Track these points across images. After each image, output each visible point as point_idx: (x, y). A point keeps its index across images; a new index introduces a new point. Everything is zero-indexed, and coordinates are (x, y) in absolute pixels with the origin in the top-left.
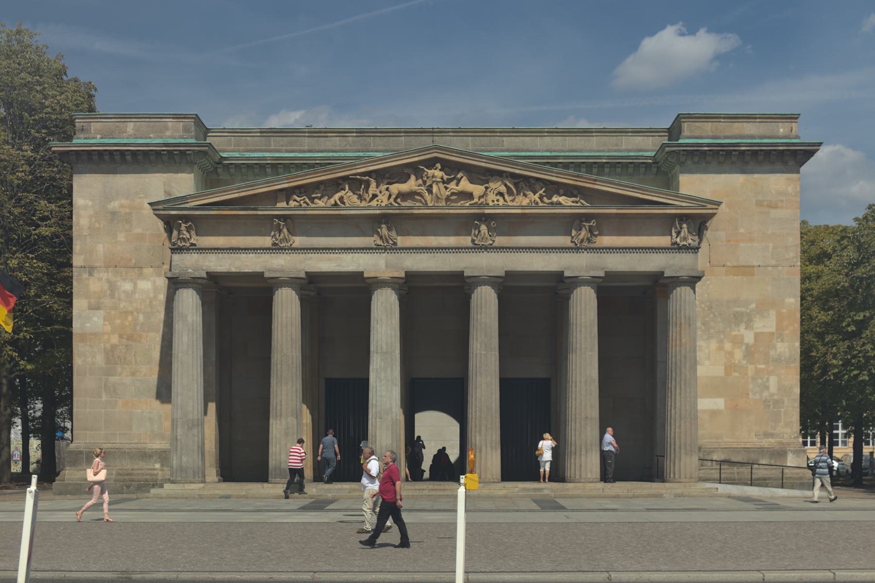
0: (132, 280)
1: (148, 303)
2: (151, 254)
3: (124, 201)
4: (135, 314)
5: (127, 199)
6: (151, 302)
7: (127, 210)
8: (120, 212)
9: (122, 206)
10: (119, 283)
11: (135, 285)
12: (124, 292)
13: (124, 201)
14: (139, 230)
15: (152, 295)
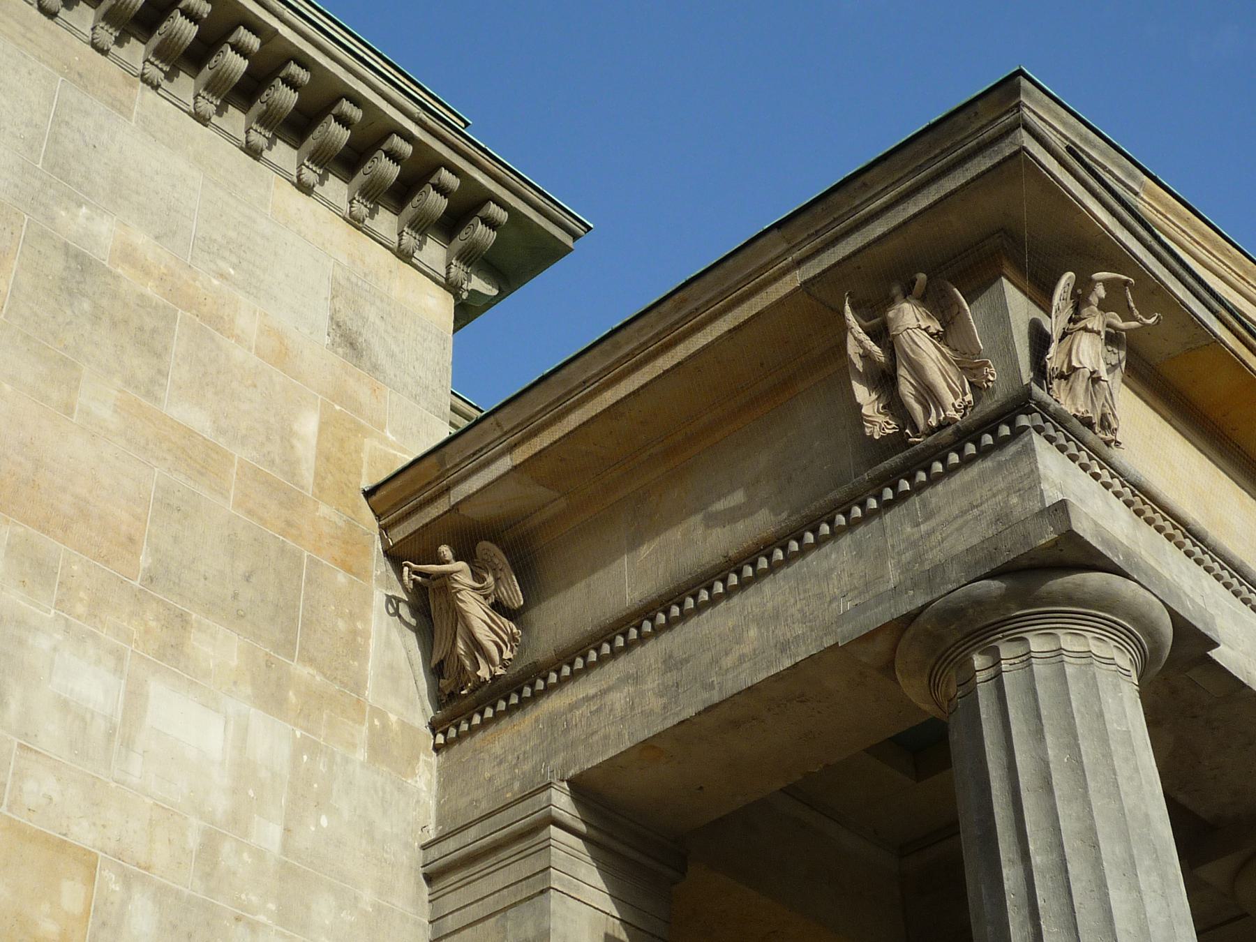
0: (119, 656)
1: (193, 841)
2: (242, 567)
3: (141, 240)
4: (109, 880)
5: (157, 238)
6: (210, 845)
7: (150, 289)
8: (117, 277)
9: (128, 255)
10: (42, 643)
11: (135, 697)
12: (64, 705)
13: (141, 240)
14: (198, 419)
15: (220, 804)
